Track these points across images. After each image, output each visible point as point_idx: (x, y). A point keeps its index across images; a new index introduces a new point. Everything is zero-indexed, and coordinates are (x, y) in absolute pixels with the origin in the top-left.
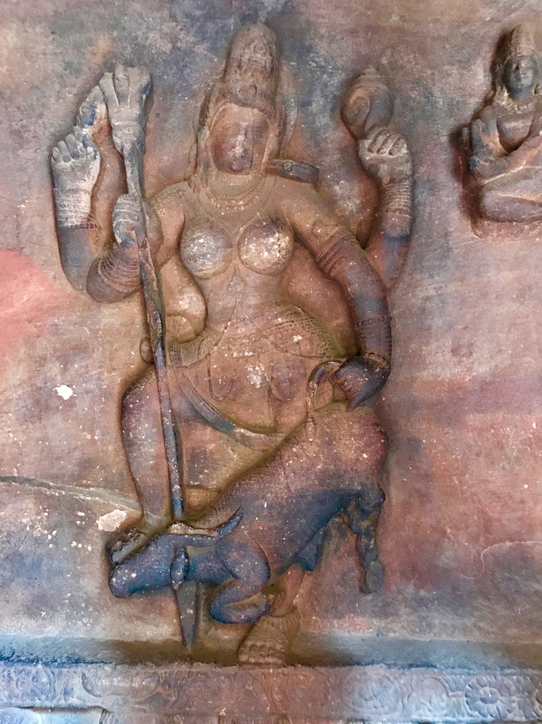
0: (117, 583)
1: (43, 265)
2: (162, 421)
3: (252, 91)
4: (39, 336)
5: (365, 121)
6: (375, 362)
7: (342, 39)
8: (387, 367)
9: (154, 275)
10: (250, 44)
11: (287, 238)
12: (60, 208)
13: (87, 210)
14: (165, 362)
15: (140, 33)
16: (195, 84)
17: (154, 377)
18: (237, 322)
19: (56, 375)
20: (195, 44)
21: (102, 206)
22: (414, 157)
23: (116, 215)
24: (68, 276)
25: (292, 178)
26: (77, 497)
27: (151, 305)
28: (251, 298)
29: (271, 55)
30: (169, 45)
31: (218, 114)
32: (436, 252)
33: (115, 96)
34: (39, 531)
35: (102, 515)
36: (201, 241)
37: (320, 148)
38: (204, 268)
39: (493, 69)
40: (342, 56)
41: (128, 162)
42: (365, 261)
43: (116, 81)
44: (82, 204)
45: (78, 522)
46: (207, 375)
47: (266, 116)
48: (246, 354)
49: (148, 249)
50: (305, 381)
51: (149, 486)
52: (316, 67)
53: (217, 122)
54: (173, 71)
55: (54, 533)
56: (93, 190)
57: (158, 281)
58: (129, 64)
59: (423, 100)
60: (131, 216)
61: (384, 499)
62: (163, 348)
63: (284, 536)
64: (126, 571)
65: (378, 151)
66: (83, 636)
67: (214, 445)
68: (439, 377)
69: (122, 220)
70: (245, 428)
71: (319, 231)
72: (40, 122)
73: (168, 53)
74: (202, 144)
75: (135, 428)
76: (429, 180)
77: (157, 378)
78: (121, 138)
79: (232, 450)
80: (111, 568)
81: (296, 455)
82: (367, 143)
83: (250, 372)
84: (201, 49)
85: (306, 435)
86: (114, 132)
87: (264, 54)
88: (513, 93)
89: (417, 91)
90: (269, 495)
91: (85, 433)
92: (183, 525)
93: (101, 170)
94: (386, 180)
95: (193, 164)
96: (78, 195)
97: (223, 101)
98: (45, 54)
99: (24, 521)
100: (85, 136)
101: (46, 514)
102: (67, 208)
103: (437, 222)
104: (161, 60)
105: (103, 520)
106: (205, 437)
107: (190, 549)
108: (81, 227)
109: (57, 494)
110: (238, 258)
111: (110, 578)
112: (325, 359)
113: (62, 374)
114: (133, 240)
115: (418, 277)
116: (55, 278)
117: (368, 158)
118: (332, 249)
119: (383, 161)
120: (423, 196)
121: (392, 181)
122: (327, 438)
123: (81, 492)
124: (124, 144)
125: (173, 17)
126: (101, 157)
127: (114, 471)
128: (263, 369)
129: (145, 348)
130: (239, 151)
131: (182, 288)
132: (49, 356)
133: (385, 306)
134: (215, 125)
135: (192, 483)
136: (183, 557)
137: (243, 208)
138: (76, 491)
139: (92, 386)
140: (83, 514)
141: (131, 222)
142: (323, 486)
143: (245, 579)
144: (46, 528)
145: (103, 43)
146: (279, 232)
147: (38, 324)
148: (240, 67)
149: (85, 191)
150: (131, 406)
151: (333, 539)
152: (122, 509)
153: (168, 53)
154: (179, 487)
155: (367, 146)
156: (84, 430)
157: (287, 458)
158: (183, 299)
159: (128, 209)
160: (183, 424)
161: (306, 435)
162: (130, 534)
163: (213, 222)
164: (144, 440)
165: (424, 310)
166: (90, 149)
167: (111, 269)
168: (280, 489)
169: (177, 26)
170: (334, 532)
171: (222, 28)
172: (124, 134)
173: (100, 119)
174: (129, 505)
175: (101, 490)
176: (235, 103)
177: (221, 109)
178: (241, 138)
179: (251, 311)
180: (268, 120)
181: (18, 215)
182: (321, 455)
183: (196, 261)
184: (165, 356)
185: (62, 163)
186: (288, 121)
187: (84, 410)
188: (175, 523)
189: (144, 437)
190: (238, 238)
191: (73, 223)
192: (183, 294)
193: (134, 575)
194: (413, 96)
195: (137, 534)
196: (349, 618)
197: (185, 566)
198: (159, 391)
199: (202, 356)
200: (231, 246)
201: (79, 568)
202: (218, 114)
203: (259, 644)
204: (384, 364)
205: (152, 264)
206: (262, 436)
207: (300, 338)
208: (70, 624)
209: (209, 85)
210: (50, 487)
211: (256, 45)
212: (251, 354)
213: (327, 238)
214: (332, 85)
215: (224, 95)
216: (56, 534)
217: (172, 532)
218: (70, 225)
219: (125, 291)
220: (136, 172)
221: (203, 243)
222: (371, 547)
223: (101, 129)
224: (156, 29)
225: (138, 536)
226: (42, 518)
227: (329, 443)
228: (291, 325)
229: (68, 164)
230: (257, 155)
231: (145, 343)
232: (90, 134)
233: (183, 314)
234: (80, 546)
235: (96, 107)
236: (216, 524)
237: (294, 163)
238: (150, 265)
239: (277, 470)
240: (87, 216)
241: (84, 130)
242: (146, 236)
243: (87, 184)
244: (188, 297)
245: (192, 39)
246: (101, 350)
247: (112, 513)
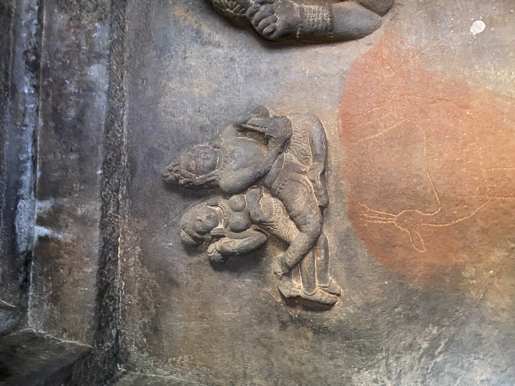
96: (305, 9)
102: (316, 19)
181: (315, 76)
185: (277, 24)
191: (327, 15)
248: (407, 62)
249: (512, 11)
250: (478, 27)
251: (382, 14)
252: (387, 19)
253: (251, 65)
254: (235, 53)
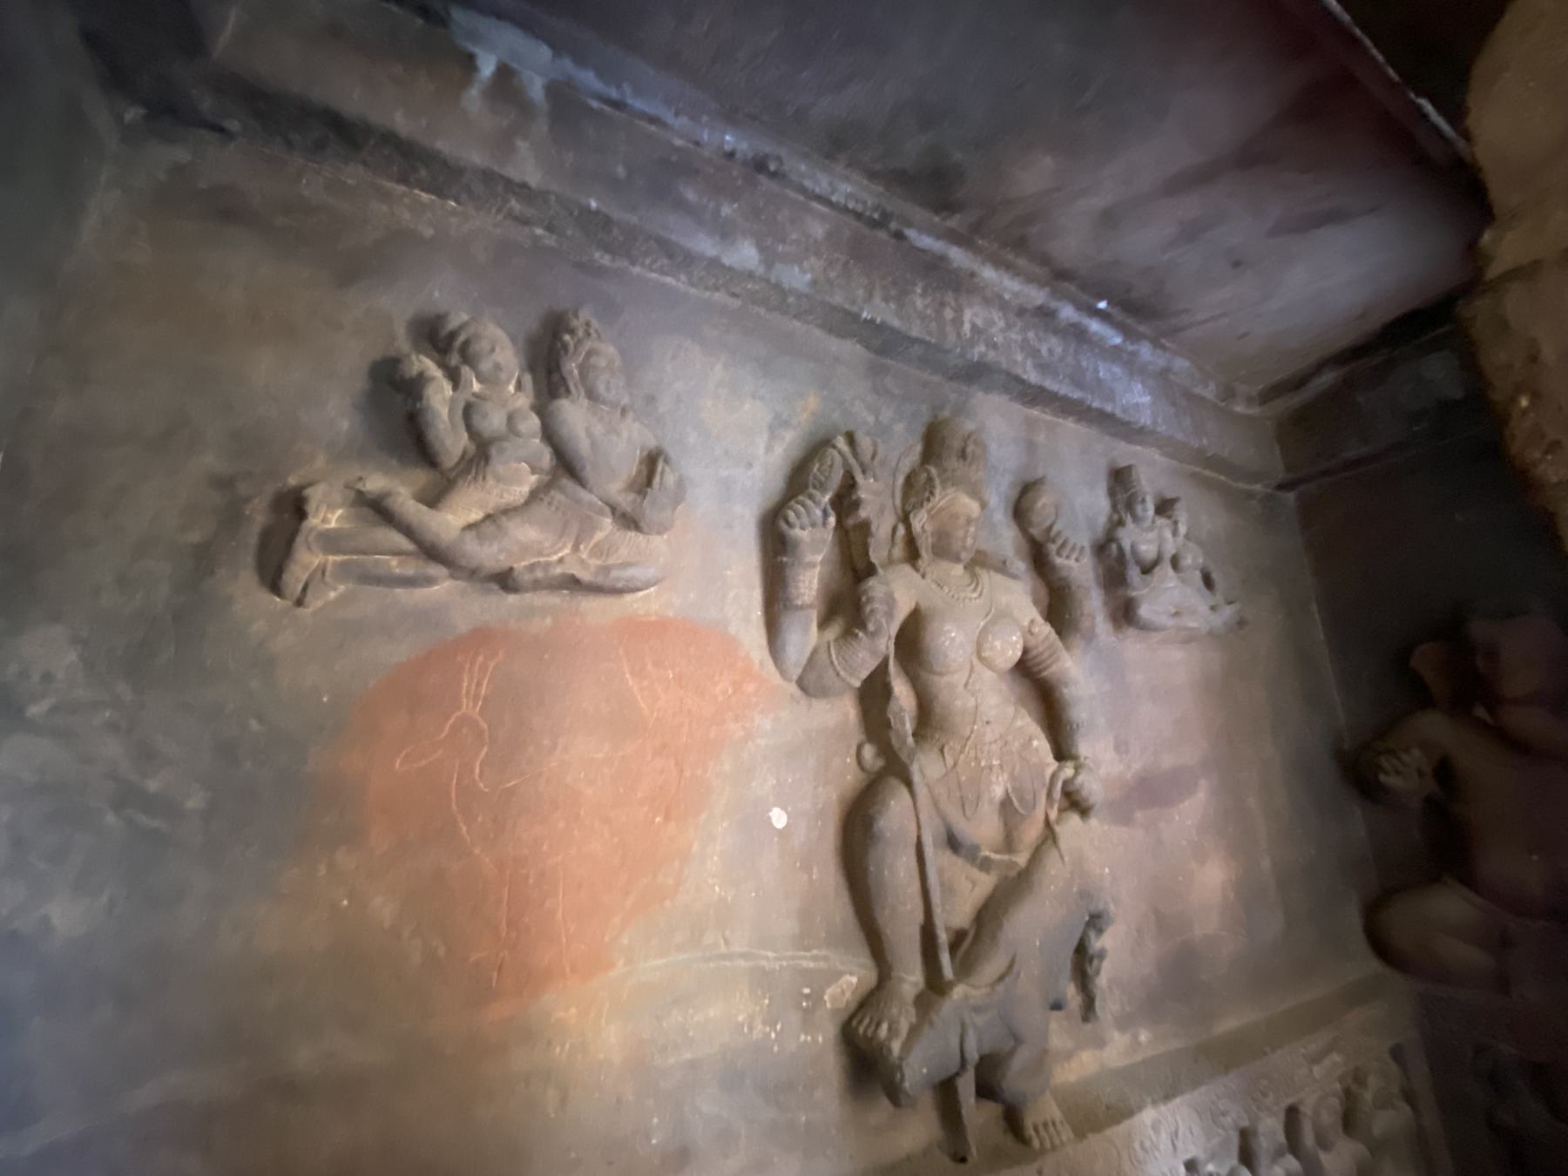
39: (1112, 493)
88: (1136, 519)
152: (851, 974)
175: (824, 952)
178: (972, 529)
210: (767, 958)
248: (736, 719)
250: (779, 818)
251: (801, 683)
252: (793, 689)
254: (757, 470)
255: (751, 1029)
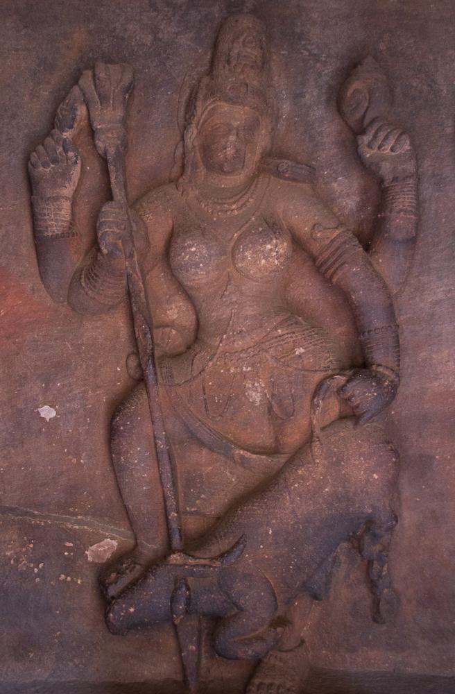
0: (114, 619)
1: (20, 276)
2: (156, 444)
3: (243, 89)
4: (18, 354)
5: (364, 117)
6: (383, 375)
7: (337, 24)
8: (396, 380)
9: (141, 285)
10: (238, 38)
11: (285, 244)
12: (39, 217)
13: (68, 218)
14: (157, 380)
15: (117, 25)
16: (178, 77)
17: (145, 396)
18: (233, 335)
19: (37, 395)
20: (178, 34)
21: (84, 211)
22: (417, 154)
23: (101, 224)
24: (47, 287)
25: (288, 179)
26: (64, 527)
27: (139, 319)
28: (247, 308)
29: (262, 48)
30: (150, 36)
31: (206, 112)
32: (444, 253)
33: (97, 96)
34: (25, 564)
35: (91, 546)
36: (194, 249)
37: (315, 142)
38: (196, 278)
40: (336, 42)
41: (112, 167)
42: (369, 267)
43: (98, 81)
44: (63, 212)
45: (66, 554)
46: (202, 393)
47: (257, 113)
48: (244, 369)
49: (135, 259)
50: (309, 397)
51: (143, 514)
52: (309, 55)
53: (205, 121)
54: (154, 64)
55: (41, 565)
56: (73, 196)
57: (145, 290)
58: (108, 60)
59: (425, 88)
60: (118, 226)
61: (397, 521)
62: (154, 366)
63: (290, 564)
64: (124, 606)
65: (379, 148)
66: (75, 679)
67: (211, 468)
68: (451, 387)
69: (108, 230)
70: (243, 449)
71: (318, 235)
72: (14, 123)
73: (149, 44)
74: (189, 142)
75: (127, 452)
76: (433, 175)
77: (149, 398)
78: (104, 142)
79: (231, 473)
80: (106, 602)
81: (303, 478)
82: (366, 139)
83: (249, 388)
84: (185, 40)
85: (312, 456)
86: (97, 136)
87: (254, 48)
89: (418, 78)
90: (274, 521)
91: (70, 457)
92: (182, 555)
93: (81, 175)
94: (388, 178)
95: (179, 164)
96: (58, 203)
97: (212, 100)
98: (17, 50)
99: (8, 553)
100: (65, 140)
101: (31, 546)
102: (47, 217)
103: (444, 220)
104: (141, 53)
105: (92, 551)
106: (199, 458)
107: (190, 580)
108: (63, 236)
109: (43, 524)
110: (232, 266)
111: (106, 615)
112: (330, 372)
113: (43, 394)
114: (120, 251)
115: (424, 279)
116: (33, 290)
117: (368, 156)
118: (333, 254)
119: (384, 159)
120: (428, 191)
121: (395, 179)
122: (334, 459)
123: (68, 520)
124: (107, 148)
125: (153, 6)
126: (82, 160)
127: (102, 497)
128: (263, 385)
129: (133, 363)
130: (230, 151)
131: (170, 297)
132: (29, 374)
133: (391, 312)
134: (203, 124)
135: (188, 509)
136: (184, 589)
137: (236, 213)
138: (63, 519)
139: (76, 405)
140: (71, 545)
141: (118, 231)
142: (332, 511)
143: (251, 611)
144: (30, 561)
145: (80, 36)
146: (277, 239)
147: (17, 340)
148: (228, 62)
149: (66, 198)
150: (122, 428)
151: (342, 565)
153: (149, 44)
154: (176, 515)
155: (366, 142)
156: (69, 453)
157: (292, 481)
158: (172, 308)
159: (114, 218)
160: (177, 446)
161: (312, 456)
162: (124, 565)
163: (204, 228)
164: (136, 465)
165: (433, 315)
166: (71, 154)
167: (96, 281)
168: (286, 514)
169: (158, 15)
170: (342, 558)
171: (206, 16)
172: (108, 137)
173: (80, 121)
174: (120, 533)
175: (89, 518)
176: (226, 101)
177: (210, 108)
178: (232, 138)
179: (248, 322)
180: (260, 117)
182: (328, 477)
183: (187, 271)
184: (156, 374)
186: (280, 115)
187: (68, 432)
188: (174, 553)
189: (136, 461)
190: (232, 244)
191: (54, 232)
192: (171, 303)
193: (132, 610)
194: (415, 84)
195: (133, 565)
196: (362, 652)
197: (187, 599)
198: (151, 412)
199: (195, 373)
200: (225, 254)
201: (68, 603)
202: (206, 112)
203: (267, 681)
204: (393, 377)
205: (139, 274)
206: (264, 457)
207: (302, 350)
208: (60, 665)
209: (193, 79)
210: (34, 516)
211: (245, 39)
212: (249, 369)
213: (327, 242)
214: (326, 74)
215: (213, 92)
216: (43, 567)
217: (171, 563)
218: (50, 234)
219: (111, 303)
220: (121, 178)
221: (195, 251)
222: (384, 573)
223: (81, 130)
224: (135, 20)
225: (134, 567)
226: (27, 550)
227: (338, 463)
228: (291, 337)
229: (48, 170)
230: (250, 155)
231: (132, 358)
232: (70, 138)
233: (171, 325)
234: (69, 579)
235: (76, 109)
236: (218, 553)
237: (290, 163)
238: (137, 274)
239: (282, 494)
240: (68, 224)
241: (65, 134)
242: (134, 246)
243: (68, 191)
244: (176, 307)
245: (175, 29)
246: (84, 366)
247: (102, 543)
249: (66, 450)
253: (7, 140)
255: (17, 561)
